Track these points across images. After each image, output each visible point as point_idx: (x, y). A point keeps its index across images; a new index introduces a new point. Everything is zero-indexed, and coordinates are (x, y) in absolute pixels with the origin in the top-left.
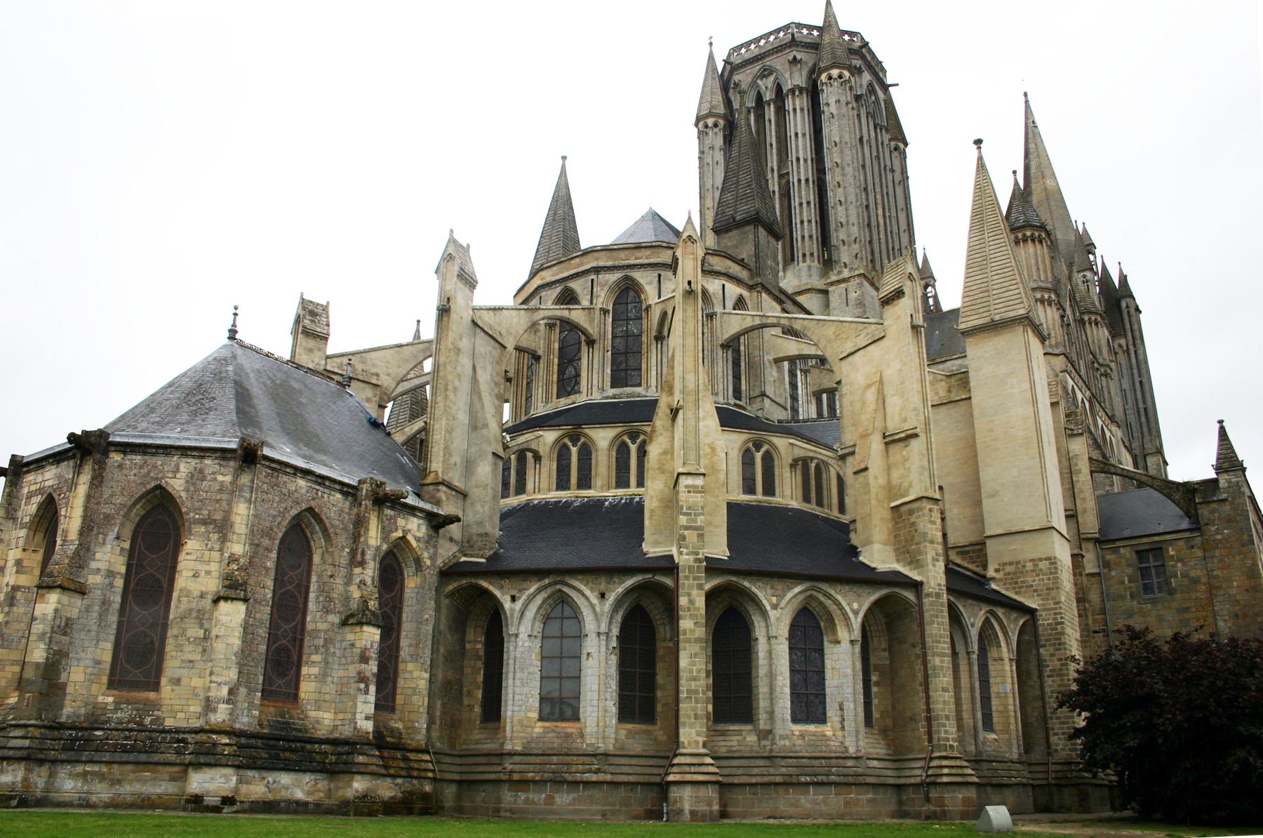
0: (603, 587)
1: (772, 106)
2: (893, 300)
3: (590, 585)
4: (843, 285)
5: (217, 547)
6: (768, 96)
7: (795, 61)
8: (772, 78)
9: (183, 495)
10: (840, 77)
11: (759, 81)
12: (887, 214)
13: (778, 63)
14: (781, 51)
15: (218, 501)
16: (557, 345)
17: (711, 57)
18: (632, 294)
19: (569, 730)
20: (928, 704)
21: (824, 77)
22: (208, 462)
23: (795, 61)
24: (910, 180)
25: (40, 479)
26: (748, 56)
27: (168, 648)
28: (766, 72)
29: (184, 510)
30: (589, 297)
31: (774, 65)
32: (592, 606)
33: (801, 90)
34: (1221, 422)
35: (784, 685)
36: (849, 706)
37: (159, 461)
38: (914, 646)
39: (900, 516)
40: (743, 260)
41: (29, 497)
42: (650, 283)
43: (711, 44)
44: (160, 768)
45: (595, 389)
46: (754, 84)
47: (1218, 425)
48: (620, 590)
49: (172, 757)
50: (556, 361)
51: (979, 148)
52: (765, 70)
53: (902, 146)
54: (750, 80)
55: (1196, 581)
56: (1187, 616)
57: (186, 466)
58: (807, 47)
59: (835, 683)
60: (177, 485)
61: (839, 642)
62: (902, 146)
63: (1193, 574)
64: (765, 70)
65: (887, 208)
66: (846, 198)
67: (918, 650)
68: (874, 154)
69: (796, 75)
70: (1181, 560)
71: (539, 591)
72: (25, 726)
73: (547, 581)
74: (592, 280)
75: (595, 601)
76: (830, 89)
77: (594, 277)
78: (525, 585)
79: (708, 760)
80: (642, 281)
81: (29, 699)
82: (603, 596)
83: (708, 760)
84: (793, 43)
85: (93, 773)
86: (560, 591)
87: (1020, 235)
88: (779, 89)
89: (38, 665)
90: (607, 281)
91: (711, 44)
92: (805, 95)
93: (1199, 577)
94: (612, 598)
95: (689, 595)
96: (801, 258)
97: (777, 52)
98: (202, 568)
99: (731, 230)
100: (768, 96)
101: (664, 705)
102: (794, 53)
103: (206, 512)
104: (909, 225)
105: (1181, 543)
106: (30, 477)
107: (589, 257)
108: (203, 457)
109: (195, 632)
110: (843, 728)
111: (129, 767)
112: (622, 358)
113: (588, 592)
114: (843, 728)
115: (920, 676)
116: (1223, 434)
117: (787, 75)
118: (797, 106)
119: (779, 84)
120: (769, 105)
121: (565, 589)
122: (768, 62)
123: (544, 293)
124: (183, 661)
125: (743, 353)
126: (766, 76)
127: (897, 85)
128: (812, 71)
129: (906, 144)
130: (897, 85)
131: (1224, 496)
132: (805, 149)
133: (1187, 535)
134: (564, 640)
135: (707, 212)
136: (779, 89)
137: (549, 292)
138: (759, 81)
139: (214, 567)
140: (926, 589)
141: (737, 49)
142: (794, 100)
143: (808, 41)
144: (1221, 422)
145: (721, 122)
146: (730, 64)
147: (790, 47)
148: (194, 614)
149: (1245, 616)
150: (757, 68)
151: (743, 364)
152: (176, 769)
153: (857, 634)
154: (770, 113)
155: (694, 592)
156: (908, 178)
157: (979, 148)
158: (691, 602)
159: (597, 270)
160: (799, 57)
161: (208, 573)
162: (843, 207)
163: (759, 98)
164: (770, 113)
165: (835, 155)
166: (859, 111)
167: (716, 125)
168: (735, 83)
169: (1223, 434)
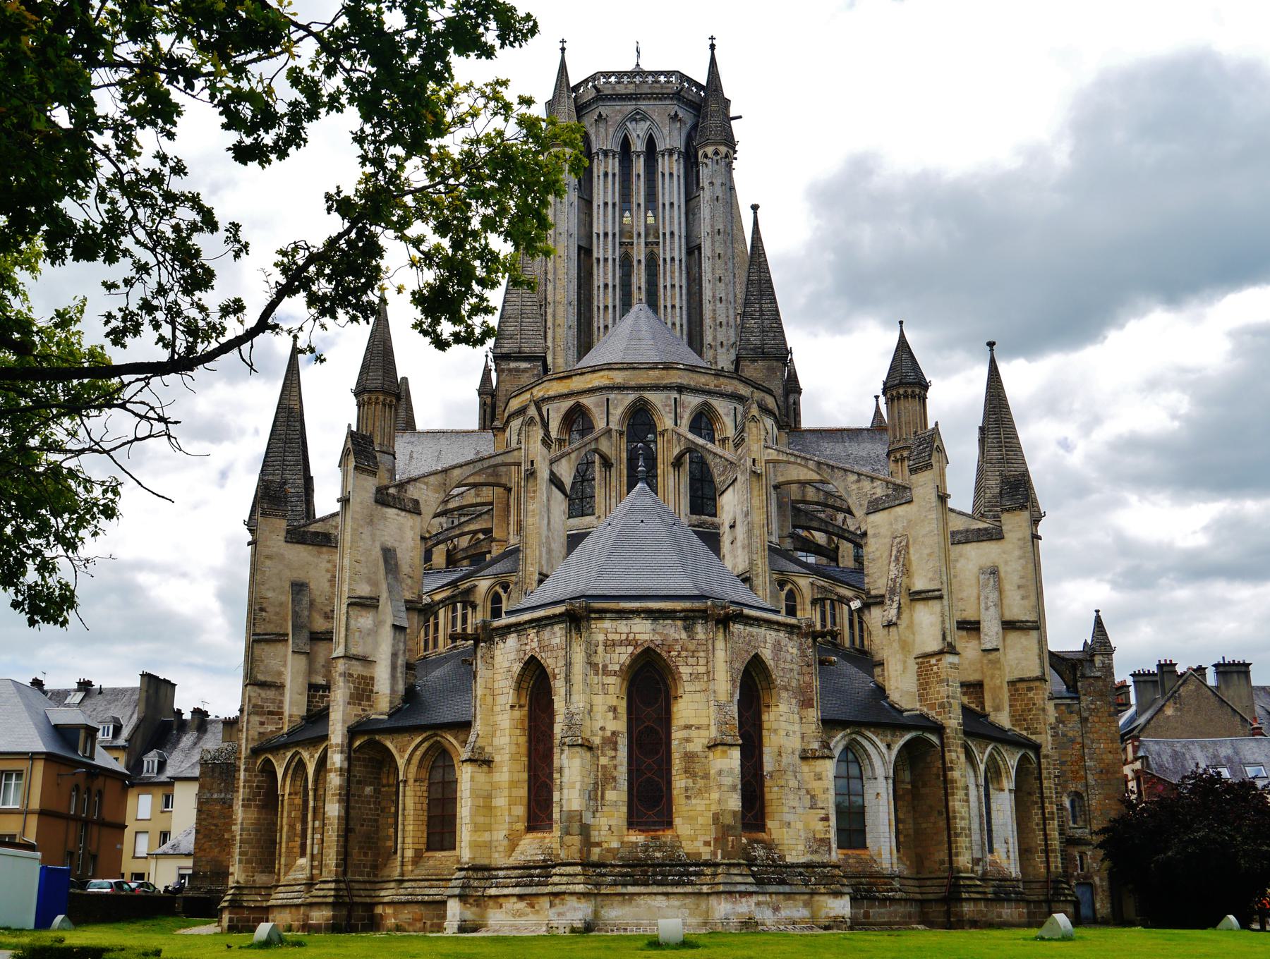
0: (889, 738)
1: (642, 159)
3: (880, 737)
5: (796, 711)
6: (638, 145)
7: (675, 118)
8: (644, 126)
9: (772, 663)
10: (716, 153)
11: (628, 123)
13: (658, 111)
14: (660, 99)
15: (792, 670)
16: (624, 455)
18: (704, 419)
19: (863, 857)
20: (1046, 840)
22: (781, 634)
23: (675, 118)
25: (625, 630)
26: (620, 89)
27: (768, 796)
28: (638, 117)
29: (774, 677)
30: (673, 416)
31: (650, 112)
32: (880, 753)
34: (1097, 611)
35: (1005, 825)
36: (1011, 840)
37: (754, 630)
38: (1030, 794)
39: (1017, 690)
41: (610, 645)
42: (727, 415)
43: (563, 49)
44: (797, 897)
45: (682, 515)
46: (622, 125)
47: (1095, 614)
48: (901, 742)
49: (803, 889)
50: (625, 472)
51: (992, 350)
52: (638, 113)
54: (619, 118)
55: (1073, 741)
56: (1064, 768)
57: (771, 636)
58: (686, 105)
59: (1001, 822)
60: (767, 654)
61: (1003, 790)
63: (1071, 734)
66: (727, 294)
67: (1036, 798)
69: (675, 133)
70: (1063, 722)
71: (843, 738)
72: (739, 865)
73: (848, 731)
74: (675, 399)
75: (884, 750)
76: (716, 167)
77: (677, 396)
78: (832, 733)
79: (978, 883)
80: (721, 411)
81: (733, 841)
82: (889, 746)
83: (978, 883)
84: (678, 96)
85: (764, 903)
86: (854, 740)
87: (909, 391)
88: (651, 143)
89: (734, 813)
90: (690, 403)
91: (563, 49)
92: (682, 160)
93: (1075, 737)
94: (895, 749)
95: (956, 751)
97: (655, 99)
98: (790, 728)
99: (756, 361)
100: (638, 145)
101: (905, 836)
103: (786, 680)
105: (1063, 708)
106: (607, 624)
107: (672, 372)
108: (779, 630)
109: (793, 783)
110: (1008, 857)
111: (781, 897)
112: (698, 485)
113: (879, 743)
114: (1008, 857)
115: (1037, 818)
116: (1099, 623)
117: (666, 131)
118: (671, 167)
120: (638, 156)
121: (859, 738)
122: (643, 105)
123: (613, 396)
124: (790, 808)
126: (636, 120)
131: (1098, 674)
133: (1068, 701)
134: (846, 780)
135: (711, 323)
136: (651, 143)
137: (619, 397)
138: (628, 123)
139: (797, 727)
140: (1044, 751)
141: (607, 75)
142: (670, 163)
144: (1097, 611)
147: (672, 99)
148: (791, 768)
149: (1108, 772)
150: (629, 107)
152: (806, 897)
153: (1012, 786)
154: (639, 166)
155: (959, 749)
157: (992, 350)
158: (958, 757)
159: (681, 389)
160: (681, 115)
161: (794, 732)
162: (723, 305)
163: (626, 143)
164: (639, 166)
165: (717, 244)
168: (600, 115)
169: (1099, 623)
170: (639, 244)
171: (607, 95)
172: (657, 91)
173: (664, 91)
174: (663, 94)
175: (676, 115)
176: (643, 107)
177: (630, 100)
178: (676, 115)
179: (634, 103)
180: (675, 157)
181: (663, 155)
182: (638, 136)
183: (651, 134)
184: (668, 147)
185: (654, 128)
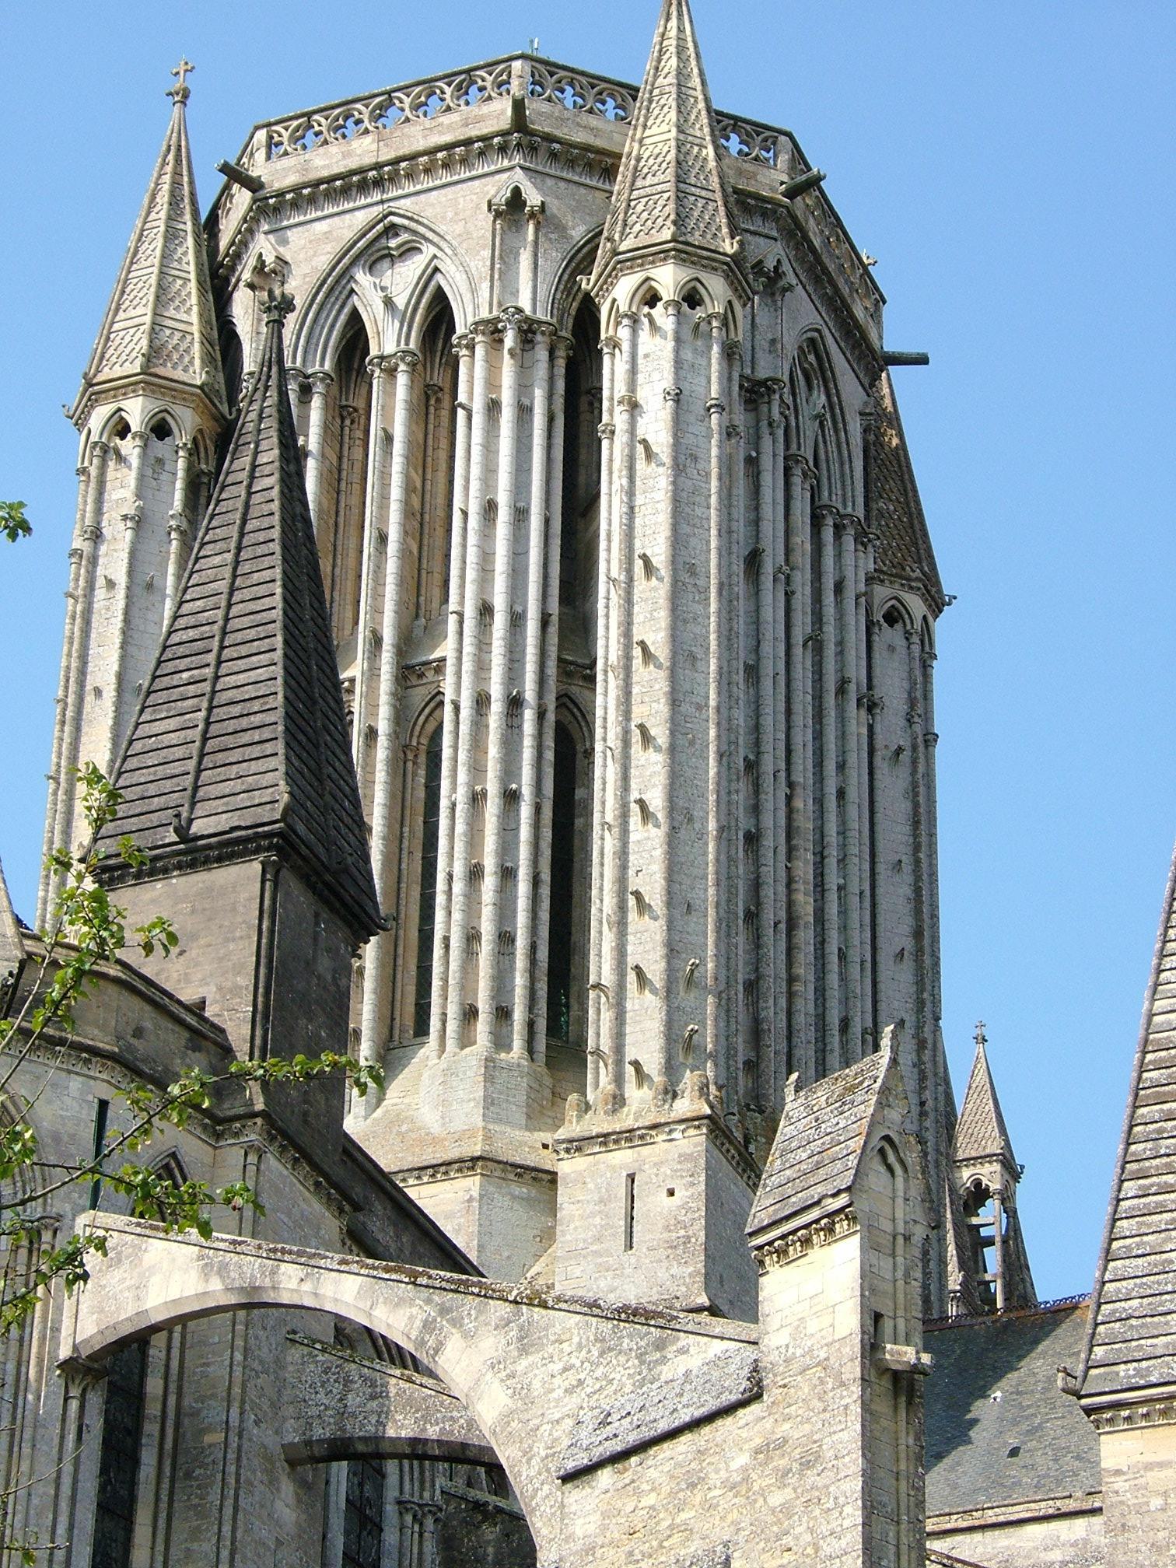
1: (402, 379)
2: (806, 1242)
4: (623, 1158)
12: (833, 880)
17: (180, 156)
21: (624, 289)
24: (940, 751)
33: (528, 331)
40: (202, 1004)
52: (392, 230)
53: (916, 605)
58: (571, 164)
62: (916, 605)
64: (392, 230)
65: (833, 853)
68: (802, 626)
92: (542, 354)
96: (452, 1026)
102: (519, 177)
104: (918, 934)
119: (440, 297)
120: (392, 372)
125: (153, 1409)
127: (922, 360)
128: (582, 260)
129: (937, 603)
130: (922, 360)
132: (517, 573)
143: (579, 137)
145: (187, 422)
146: (253, 185)
147: (503, 149)
151: (148, 1458)
156: (930, 739)
160: (533, 197)
163: (355, 339)
166: (756, 442)
167: (160, 429)
168: (261, 262)
170: (373, 673)
171: (280, 194)
172: (448, 138)
173: (474, 132)
174: (468, 142)
175: (516, 200)
176: (405, 205)
177: (364, 187)
178: (516, 200)
179: (377, 196)
180: (509, 339)
181: (471, 347)
182: (388, 303)
183: (439, 291)
184: (485, 314)
185: (447, 265)
